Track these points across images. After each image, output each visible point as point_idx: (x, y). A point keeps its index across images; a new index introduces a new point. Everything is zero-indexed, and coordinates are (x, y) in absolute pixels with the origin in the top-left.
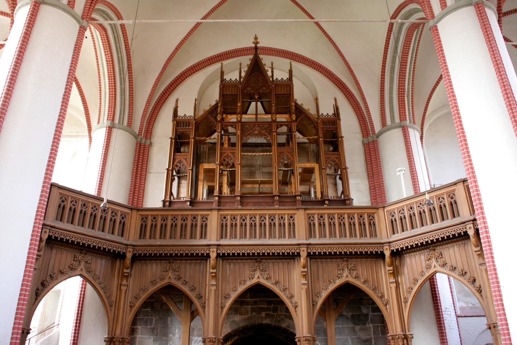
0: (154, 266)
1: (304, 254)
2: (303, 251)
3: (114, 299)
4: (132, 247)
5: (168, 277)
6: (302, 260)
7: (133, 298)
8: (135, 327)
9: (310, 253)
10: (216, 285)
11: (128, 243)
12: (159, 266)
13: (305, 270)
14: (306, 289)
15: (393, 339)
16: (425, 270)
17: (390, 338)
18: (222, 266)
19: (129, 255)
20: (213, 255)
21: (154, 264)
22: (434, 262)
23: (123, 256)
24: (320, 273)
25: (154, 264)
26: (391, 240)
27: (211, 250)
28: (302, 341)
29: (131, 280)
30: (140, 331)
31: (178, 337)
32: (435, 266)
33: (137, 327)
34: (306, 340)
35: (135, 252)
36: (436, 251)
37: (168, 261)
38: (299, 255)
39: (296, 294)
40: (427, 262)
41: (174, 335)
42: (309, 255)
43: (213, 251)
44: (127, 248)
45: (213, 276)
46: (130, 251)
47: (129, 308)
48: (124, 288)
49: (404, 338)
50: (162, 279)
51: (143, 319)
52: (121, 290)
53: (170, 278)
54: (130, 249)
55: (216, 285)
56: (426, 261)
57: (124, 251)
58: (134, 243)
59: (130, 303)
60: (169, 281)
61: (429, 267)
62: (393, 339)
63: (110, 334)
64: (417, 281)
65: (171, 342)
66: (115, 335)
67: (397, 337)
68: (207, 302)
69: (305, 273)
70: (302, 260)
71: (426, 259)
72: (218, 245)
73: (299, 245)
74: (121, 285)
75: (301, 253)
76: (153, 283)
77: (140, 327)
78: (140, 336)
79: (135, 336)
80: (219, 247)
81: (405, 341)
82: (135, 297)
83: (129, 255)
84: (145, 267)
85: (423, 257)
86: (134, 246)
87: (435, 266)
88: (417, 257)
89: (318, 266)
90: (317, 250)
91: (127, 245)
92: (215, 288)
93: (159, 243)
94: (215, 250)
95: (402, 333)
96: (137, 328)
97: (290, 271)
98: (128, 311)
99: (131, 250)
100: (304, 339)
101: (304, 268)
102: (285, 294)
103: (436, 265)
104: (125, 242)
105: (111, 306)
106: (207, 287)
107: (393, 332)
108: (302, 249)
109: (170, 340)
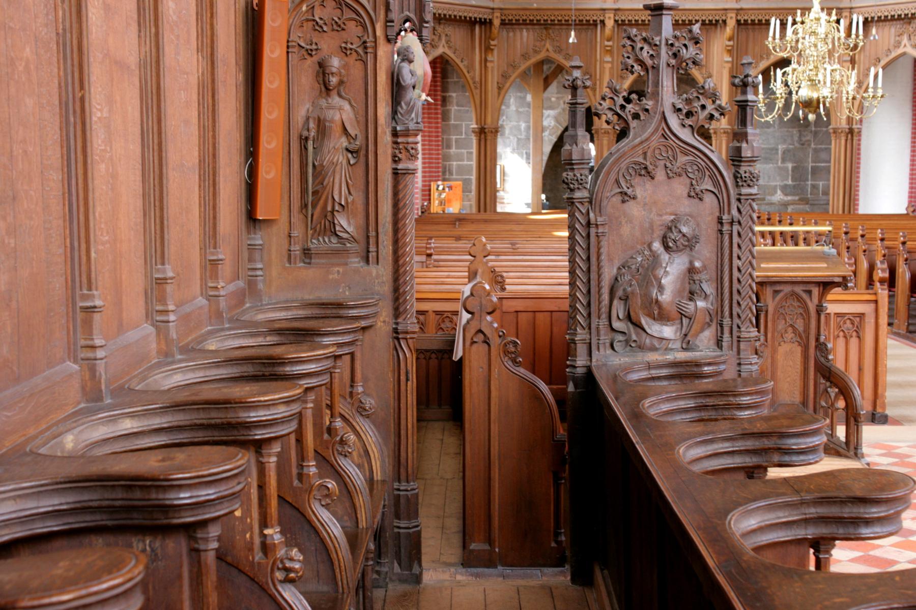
0: (525, 33)
1: (731, 23)
2: (731, 18)
3: (477, 79)
4: (499, 11)
5: (545, 49)
6: (729, 30)
7: (500, 77)
8: (448, 94)
9: (740, 20)
10: (612, 63)
11: (496, 6)
12: (531, 33)
13: (731, 43)
14: (730, 68)
15: (835, 132)
16: (891, 48)
17: (831, 131)
18: (618, 34)
19: (497, 22)
20: (610, 23)
21: (525, 30)
22: (905, 40)
23: (486, 23)
24: (750, 45)
25: (525, 30)
26: (854, 5)
27: (607, 15)
28: (718, 133)
29: (495, 52)
30: (455, 101)
31: (514, 109)
32: (905, 46)
33: (450, 94)
34: (725, 133)
35: (503, 18)
36: (911, 25)
37: (542, 27)
38: (724, 22)
39: (715, 73)
40: (897, 38)
41: (508, 106)
42: (738, 22)
43: (609, 18)
44: (493, 13)
45: (607, 51)
46: (497, 17)
47: (496, 90)
48: (489, 64)
49: (849, 132)
50: (536, 52)
51: (458, 82)
52: (486, 66)
53: (548, 50)
54: (497, 14)
55: (612, 63)
56: (895, 36)
57: (490, 17)
58: (503, 7)
59: (498, 83)
60: (547, 54)
61: (898, 44)
62: (835, 132)
63: (479, 122)
64: (879, 61)
65: (504, 118)
66: (485, 124)
67: (840, 131)
68: (598, 83)
69: (730, 48)
70: (729, 30)
71: (897, 34)
72: (616, 10)
73: (726, 10)
74: (486, 60)
75: (728, 21)
76: (525, 56)
77: (454, 95)
78: (456, 108)
79: (448, 108)
80: (618, 12)
81: (849, 136)
82: (502, 76)
83: (497, 22)
84: (511, 34)
85: (893, 30)
86: (501, 9)
87: (905, 46)
88: (886, 29)
89: (747, 38)
90: (749, 17)
91: (493, 9)
92: (609, 65)
93: (535, 5)
94: (612, 16)
95: (848, 127)
96: (449, 96)
97: (710, 41)
98: (496, 94)
99: (499, 15)
100: (722, 131)
101: (730, 40)
102: (701, 73)
103: (907, 45)
104: (491, 5)
105: (476, 88)
106: (598, 63)
107: (836, 124)
108: (729, 15)
109: (503, 115)
